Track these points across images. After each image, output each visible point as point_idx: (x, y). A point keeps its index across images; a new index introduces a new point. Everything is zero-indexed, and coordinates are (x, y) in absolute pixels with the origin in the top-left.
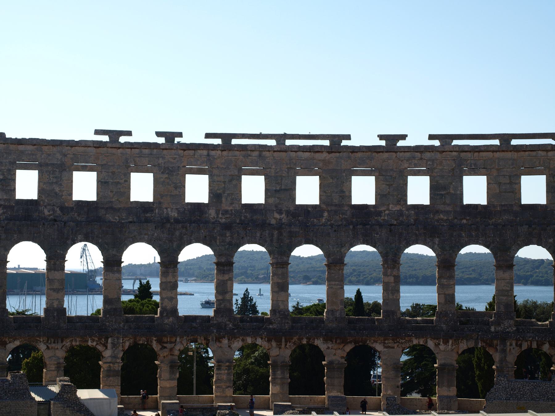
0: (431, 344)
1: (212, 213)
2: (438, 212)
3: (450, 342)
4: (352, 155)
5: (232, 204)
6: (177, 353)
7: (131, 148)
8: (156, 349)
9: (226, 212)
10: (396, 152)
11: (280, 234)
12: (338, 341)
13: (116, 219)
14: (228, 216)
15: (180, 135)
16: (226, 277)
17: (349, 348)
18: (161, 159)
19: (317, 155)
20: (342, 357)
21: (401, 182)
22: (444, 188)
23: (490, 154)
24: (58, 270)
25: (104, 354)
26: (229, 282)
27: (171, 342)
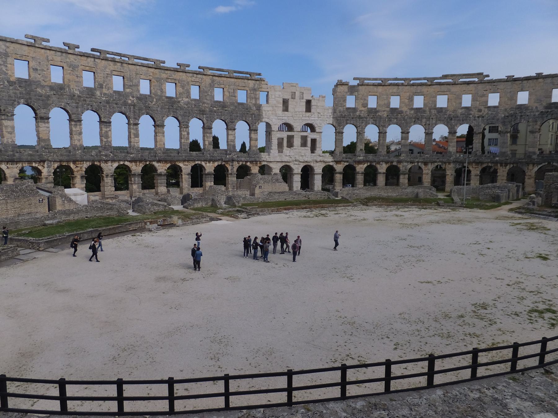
0: (203, 163)
1: (98, 93)
2: (204, 103)
3: (211, 162)
4: (166, 72)
5: (108, 90)
6: (84, 170)
7: (50, 50)
8: (73, 168)
9: (105, 94)
10: (186, 72)
11: (134, 108)
12: (164, 162)
13: (43, 92)
14: (107, 96)
15: (78, 47)
16: (108, 129)
17: (168, 165)
18: (68, 59)
19: (150, 69)
20: (165, 170)
21: (188, 87)
22: (207, 92)
23: (225, 79)
24: (10, 120)
25: (43, 171)
26: (109, 132)
27: (81, 164)
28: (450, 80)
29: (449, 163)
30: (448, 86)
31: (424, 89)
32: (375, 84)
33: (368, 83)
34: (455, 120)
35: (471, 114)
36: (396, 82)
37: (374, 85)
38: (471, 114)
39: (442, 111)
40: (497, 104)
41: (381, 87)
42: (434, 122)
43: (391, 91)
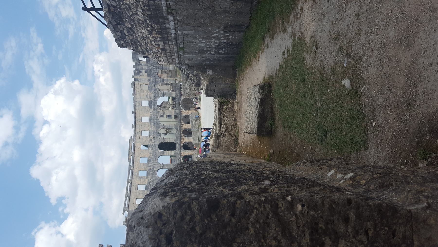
28: (132, 157)
29: (181, 153)
30: (135, 157)
31: (135, 170)
32: (129, 200)
33: (127, 204)
34: (156, 152)
35: (153, 144)
36: (129, 187)
37: (129, 201)
38: (153, 144)
39: (150, 160)
40: (148, 132)
41: (131, 196)
42: (156, 163)
43: (134, 190)
